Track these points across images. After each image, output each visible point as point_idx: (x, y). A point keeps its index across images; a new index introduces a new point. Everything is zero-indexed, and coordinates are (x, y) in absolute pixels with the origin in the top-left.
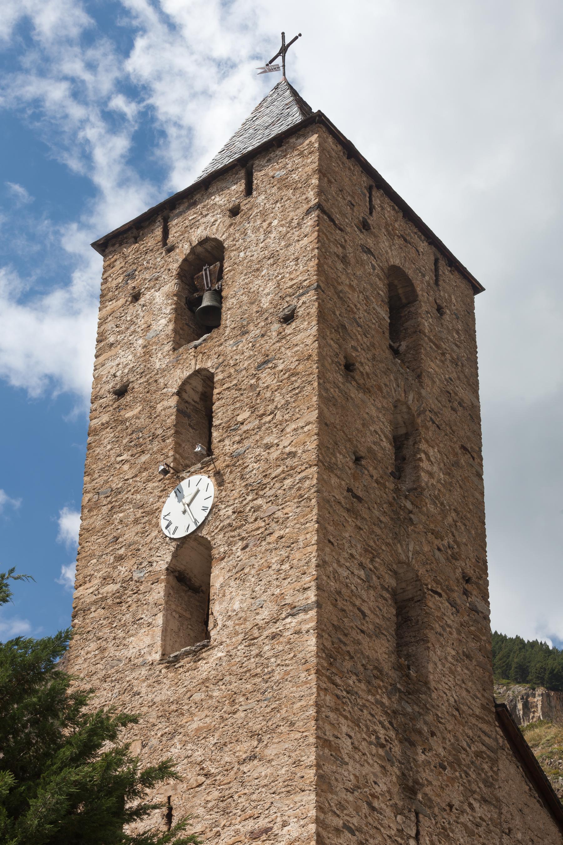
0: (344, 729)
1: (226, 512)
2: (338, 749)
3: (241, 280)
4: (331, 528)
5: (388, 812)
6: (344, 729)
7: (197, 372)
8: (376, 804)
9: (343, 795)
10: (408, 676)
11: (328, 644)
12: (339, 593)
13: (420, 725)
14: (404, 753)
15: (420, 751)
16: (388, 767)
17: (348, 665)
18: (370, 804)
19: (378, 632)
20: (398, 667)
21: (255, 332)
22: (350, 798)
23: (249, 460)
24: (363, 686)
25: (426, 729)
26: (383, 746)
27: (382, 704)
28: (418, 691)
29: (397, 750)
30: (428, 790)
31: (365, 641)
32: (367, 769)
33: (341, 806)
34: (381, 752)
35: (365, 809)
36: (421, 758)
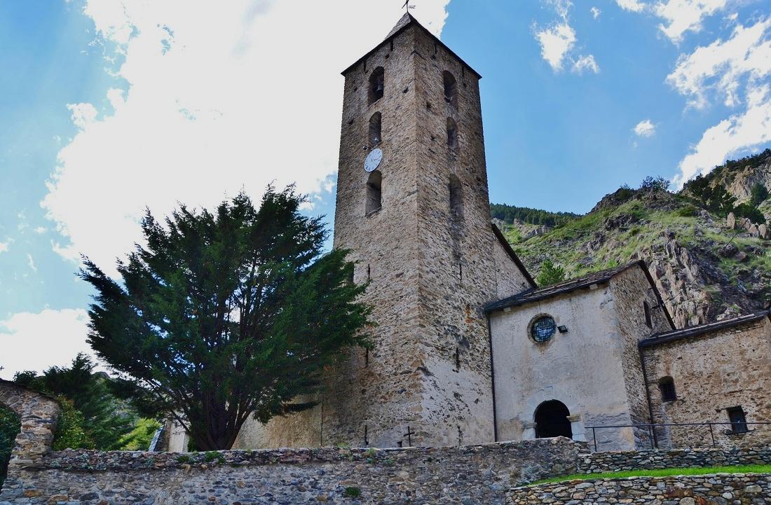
0: (430, 235)
1: (386, 161)
2: (427, 243)
3: (389, 80)
4: (422, 163)
5: (449, 265)
6: (430, 235)
7: (376, 113)
8: (443, 262)
9: (429, 259)
10: (456, 215)
11: (422, 205)
12: (426, 186)
13: (461, 233)
14: (455, 243)
15: (461, 242)
16: (448, 248)
17: (431, 212)
18: (441, 262)
19: (443, 200)
20: (451, 212)
21: (394, 97)
22: (433, 260)
23: (393, 142)
24: (437, 219)
25: (463, 234)
26: (445, 241)
27: (445, 226)
28: (460, 221)
29: (451, 242)
30: (465, 256)
31: (438, 203)
32: (439, 250)
33: (429, 263)
34: (445, 243)
35: (439, 264)
36: (461, 245)
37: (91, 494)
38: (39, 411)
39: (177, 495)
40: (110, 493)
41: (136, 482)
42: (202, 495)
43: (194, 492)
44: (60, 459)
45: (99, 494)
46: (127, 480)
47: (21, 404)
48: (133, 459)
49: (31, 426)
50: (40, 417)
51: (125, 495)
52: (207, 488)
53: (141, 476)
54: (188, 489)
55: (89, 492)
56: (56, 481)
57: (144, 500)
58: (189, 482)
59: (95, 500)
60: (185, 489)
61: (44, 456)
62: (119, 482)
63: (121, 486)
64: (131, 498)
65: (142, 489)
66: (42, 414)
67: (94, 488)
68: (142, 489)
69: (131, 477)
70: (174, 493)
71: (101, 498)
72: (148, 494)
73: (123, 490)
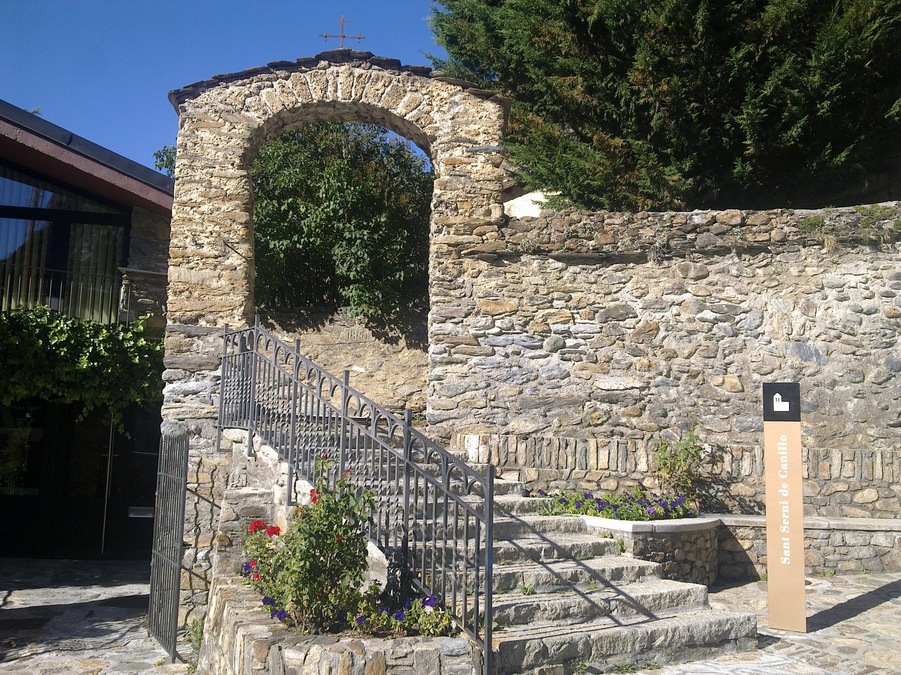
37: (616, 308)
38: (472, 127)
39: (808, 308)
40: (658, 306)
41: (712, 278)
42: (866, 304)
43: (845, 299)
44: (535, 232)
45: (637, 306)
46: (692, 274)
47: (428, 113)
48: (695, 229)
49: (462, 163)
50: (476, 139)
51: (695, 309)
52: (877, 288)
53: (721, 265)
54: (834, 291)
55: (612, 304)
56: (538, 279)
57: (737, 318)
58: (833, 276)
59: (630, 322)
60: (827, 291)
61: (500, 227)
62: (676, 280)
63: (682, 290)
64: (708, 315)
65: (730, 292)
66: (478, 134)
67: (625, 296)
68: (730, 292)
69: (701, 269)
70: (802, 301)
71: (645, 317)
72: (744, 306)
73: (686, 296)
